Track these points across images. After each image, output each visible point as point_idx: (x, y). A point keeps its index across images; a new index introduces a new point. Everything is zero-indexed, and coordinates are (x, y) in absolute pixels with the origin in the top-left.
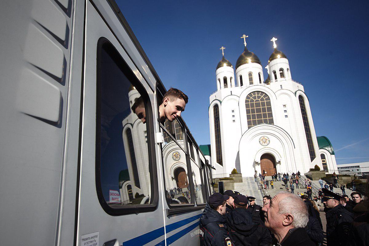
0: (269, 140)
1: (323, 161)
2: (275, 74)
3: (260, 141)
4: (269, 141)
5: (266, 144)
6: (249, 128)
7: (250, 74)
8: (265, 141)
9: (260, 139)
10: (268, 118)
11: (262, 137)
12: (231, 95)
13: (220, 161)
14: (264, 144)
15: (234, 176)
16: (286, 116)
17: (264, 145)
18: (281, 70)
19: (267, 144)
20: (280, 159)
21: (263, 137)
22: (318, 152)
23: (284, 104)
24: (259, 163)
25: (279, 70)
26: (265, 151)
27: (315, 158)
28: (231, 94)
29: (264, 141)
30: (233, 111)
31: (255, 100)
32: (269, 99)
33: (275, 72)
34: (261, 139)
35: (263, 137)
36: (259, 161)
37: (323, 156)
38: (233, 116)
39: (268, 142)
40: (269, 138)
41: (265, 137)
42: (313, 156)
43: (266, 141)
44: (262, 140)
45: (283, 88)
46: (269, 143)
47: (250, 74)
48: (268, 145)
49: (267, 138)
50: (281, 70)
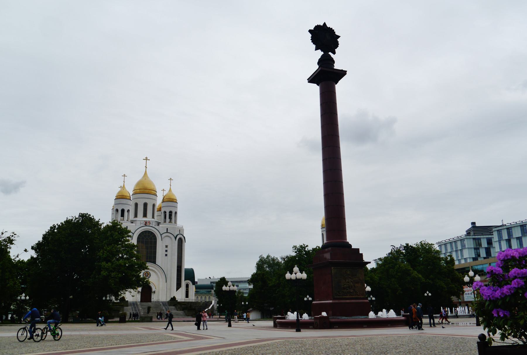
1: (186, 289)
4: (150, 275)
7: (145, 205)
10: (152, 260)
16: (166, 255)
18: (171, 212)
20: (155, 290)
22: (184, 283)
25: (168, 212)
27: (180, 288)
31: (145, 238)
34: (145, 273)
37: (187, 286)
39: (149, 276)
42: (179, 286)
43: (148, 276)
44: (145, 274)
45: (168, 232)
46: (150, 277)
47: (145, 205)
49: (149, 273)
50: (171, 212)
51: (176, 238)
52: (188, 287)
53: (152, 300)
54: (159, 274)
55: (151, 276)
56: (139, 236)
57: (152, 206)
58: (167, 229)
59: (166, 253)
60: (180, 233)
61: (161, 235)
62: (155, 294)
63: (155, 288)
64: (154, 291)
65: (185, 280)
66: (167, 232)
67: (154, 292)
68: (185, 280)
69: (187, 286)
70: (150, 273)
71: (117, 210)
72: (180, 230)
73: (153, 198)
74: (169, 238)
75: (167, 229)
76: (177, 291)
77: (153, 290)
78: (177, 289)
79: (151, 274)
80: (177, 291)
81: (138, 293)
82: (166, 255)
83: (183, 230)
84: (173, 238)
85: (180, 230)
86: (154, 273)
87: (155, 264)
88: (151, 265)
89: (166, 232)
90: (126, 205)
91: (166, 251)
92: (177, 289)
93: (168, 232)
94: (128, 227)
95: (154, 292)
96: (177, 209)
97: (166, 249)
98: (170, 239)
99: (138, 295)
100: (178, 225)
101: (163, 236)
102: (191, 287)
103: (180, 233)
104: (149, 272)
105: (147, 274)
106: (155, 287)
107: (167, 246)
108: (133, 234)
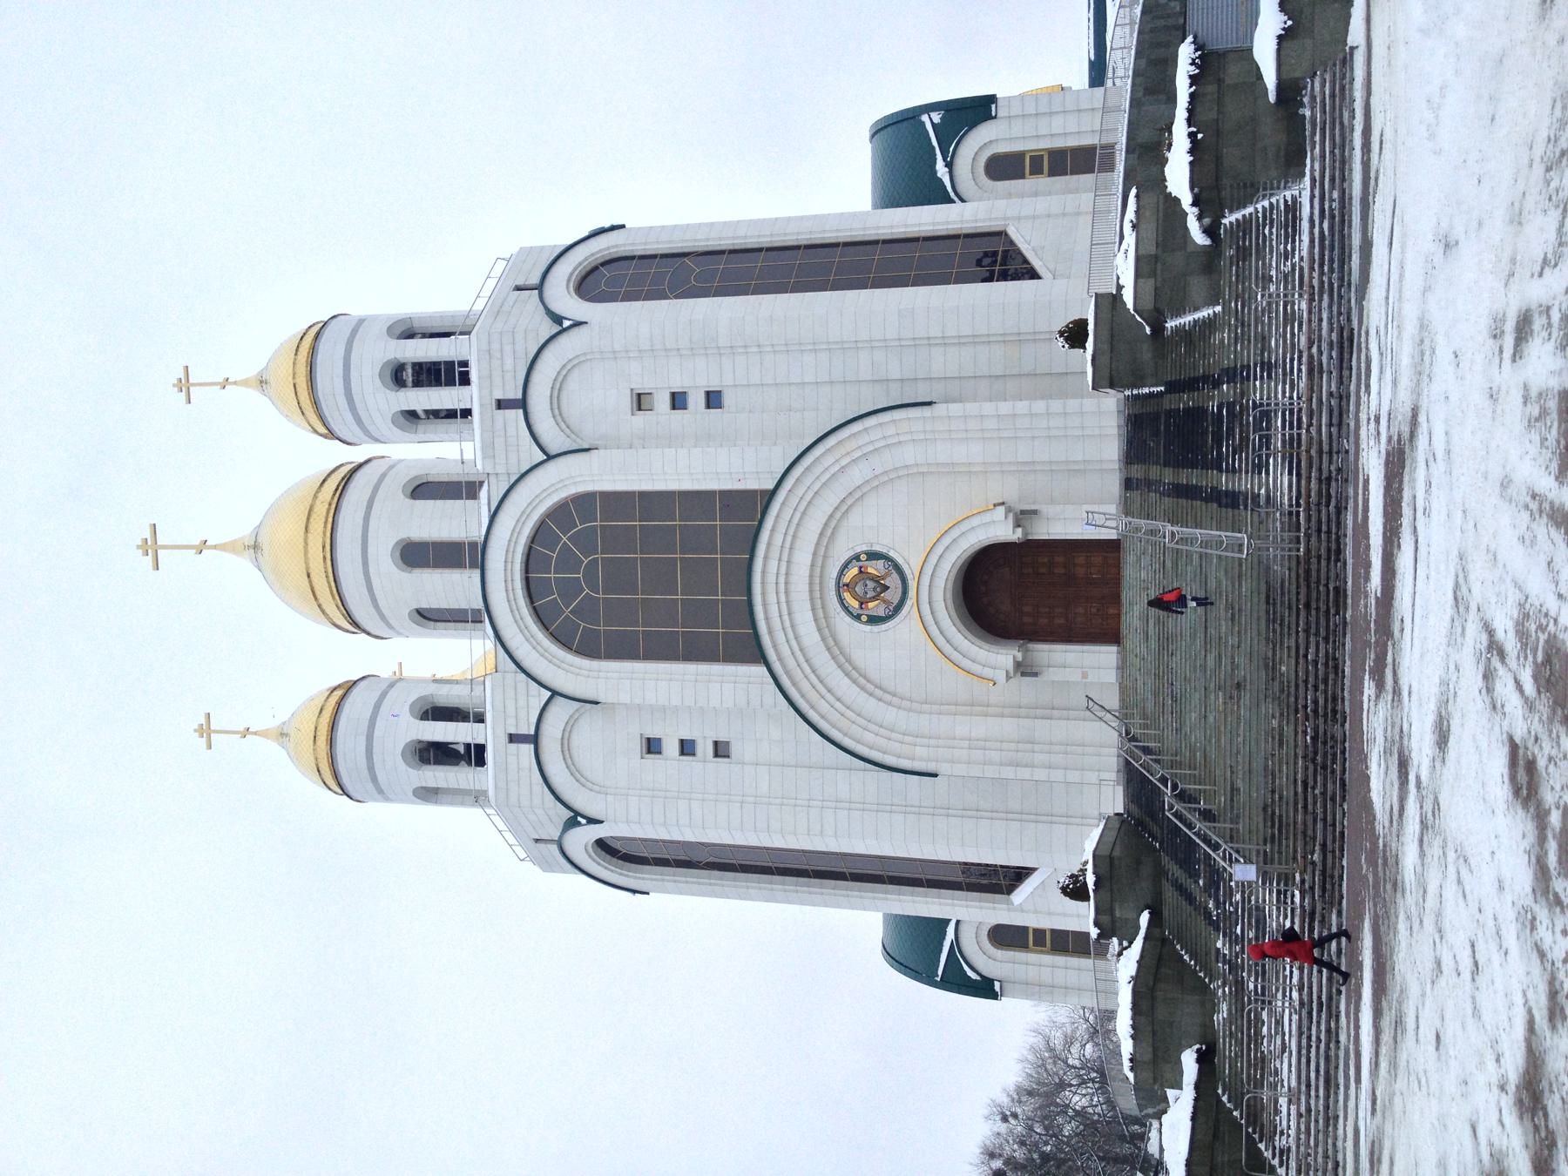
0: (863, 557)
1: (1036, 170)
2: (422, 415)
3: (874, 620)
4: (873, 556)
5: (893, 581)
7: (415, 555)
8: (871, 584)
9: (858, 618)
11: (841, 600)
12: (535, 739)
14: (893, 595)
15: (1112, 914)
17: (900, 591)
18: (398, 375)
19: (895, 575)
21: (847, 596)
23: (627, 402)
24: (1019, 656)
26: (940, 605)
28: (528, 749)
30: (652, 746)
32: (584, 503)
33: (412, 415)
34: (855, 604)
35: (847, 596)
36: (1003, 657)
37: (1004, 167)
38: (687, 748)
39: (875, 568)
40: (852, 553)
41: (846, 579)
43: (876, 579)
47: (415, 555)
48: (898, 568)
49: (853, 571)
50: (398, 375)
52: (1019, 156)
53: (1112, 535)
54: (857, 475)
55: (884, 550)
56: (566, 644)
57: (420, 503)
58: (501, 404)
59: (696, 400)
61: (550, 458)
62: (1046, 509)
63: (987, 517)
64: (1017, 525)
65: (937, 195)
66: (522, 404)
67: (1022, 517)
69: (1004, 167)
70: (857, 558)
71: (428, 794)
72: (518, 288)
74: (573, 384)
75: (501, 404)
76: (1033, 275)
77: (1003, 531)
79: (865, 548)
81: (1035, 674)
82: (713, 399)
83: (527, 252)
84: (569, 345)
85: (518, 288)
86: (854, 519)
88: (775, 554)
89: (520, 412)
90: (377, 733)
93: (519, 396)
94: (513, 731)
95: (1022, 517)
96: (375, 318)
97: (662, 402)
98: (575, 375)
99: (1051, 675)
100: (479, 306)
101: (554, 438)
102: (1018, 129)
104: (846, 566)
106: (976, 521)
108: (555, 693)
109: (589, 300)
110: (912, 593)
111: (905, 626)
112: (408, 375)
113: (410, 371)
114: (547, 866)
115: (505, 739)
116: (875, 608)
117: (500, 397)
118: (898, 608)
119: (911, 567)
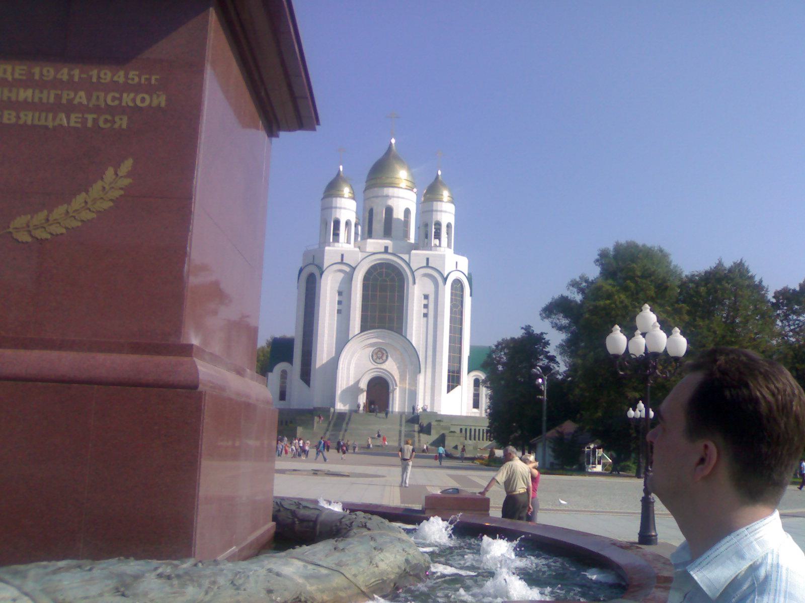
5: (381, 361)
6: (364, 328)
8: (380, 356)
9: (373, 352)
13: (306, 375)
14: (378, 361)
17: (378, 362)
21: (378, 349)
29: (379, 355)
39: (384, 358)
43: (381, 358)
51: (445, 280)
60: (458, 269)
61: (413, 273)
66: (427, 266)
68: (469, 372)
72: (457, 262)
73: (400, 196)
75: (428, 259)
76: (448, 391)
78: (450, 388)
80: (448, 391)
85: (457, 262)
87: (402, 335)
91: (426, 306)
92: (450, 388)
103: (456, 268)
104: (385, 350)
105: (380, 353)
107: (426, 297)
109: (452, 283)
110: (378, 365)
111: (371, 365)
112: (437, 227)
113: (439, 227)
114: (306, 254)
115: (342, 253)
116: (374, 357)
117: (430, 260)
118: (376, 363)
119: (384, 366)
